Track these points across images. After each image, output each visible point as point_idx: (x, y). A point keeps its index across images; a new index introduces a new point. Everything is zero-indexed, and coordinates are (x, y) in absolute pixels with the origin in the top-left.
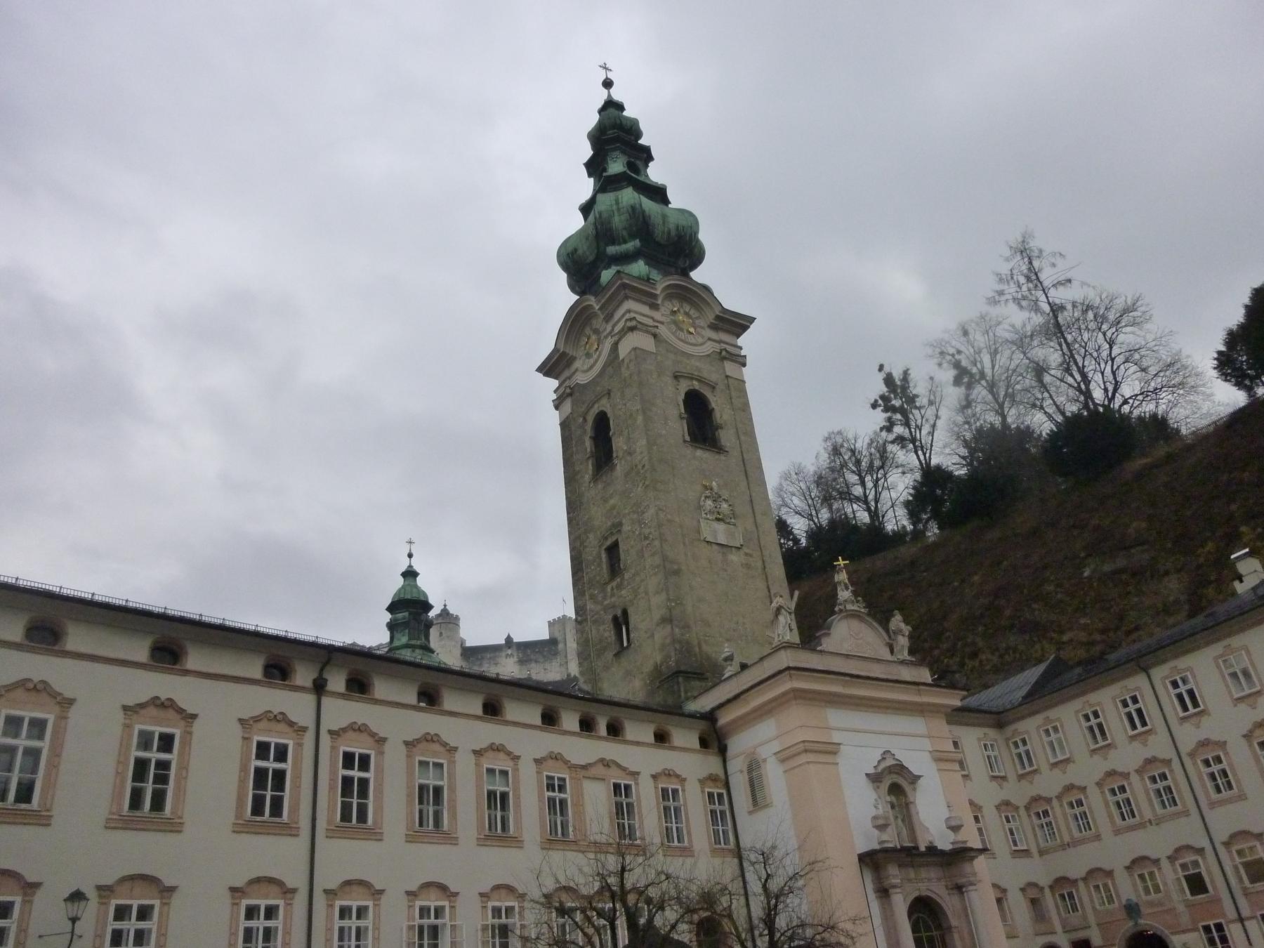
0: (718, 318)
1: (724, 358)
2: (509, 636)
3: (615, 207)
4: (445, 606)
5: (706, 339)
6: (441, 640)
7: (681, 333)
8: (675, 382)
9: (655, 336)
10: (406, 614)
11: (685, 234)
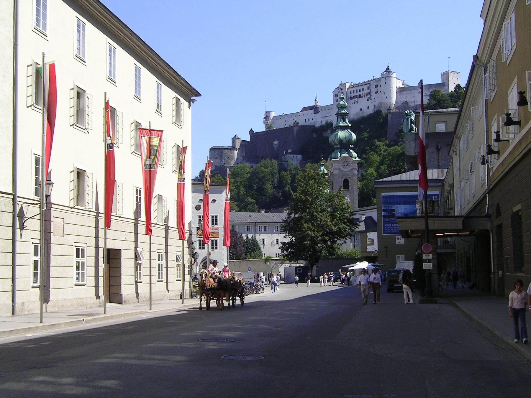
0: (352, 162)
4: (388, 66)
9: (339, 170)
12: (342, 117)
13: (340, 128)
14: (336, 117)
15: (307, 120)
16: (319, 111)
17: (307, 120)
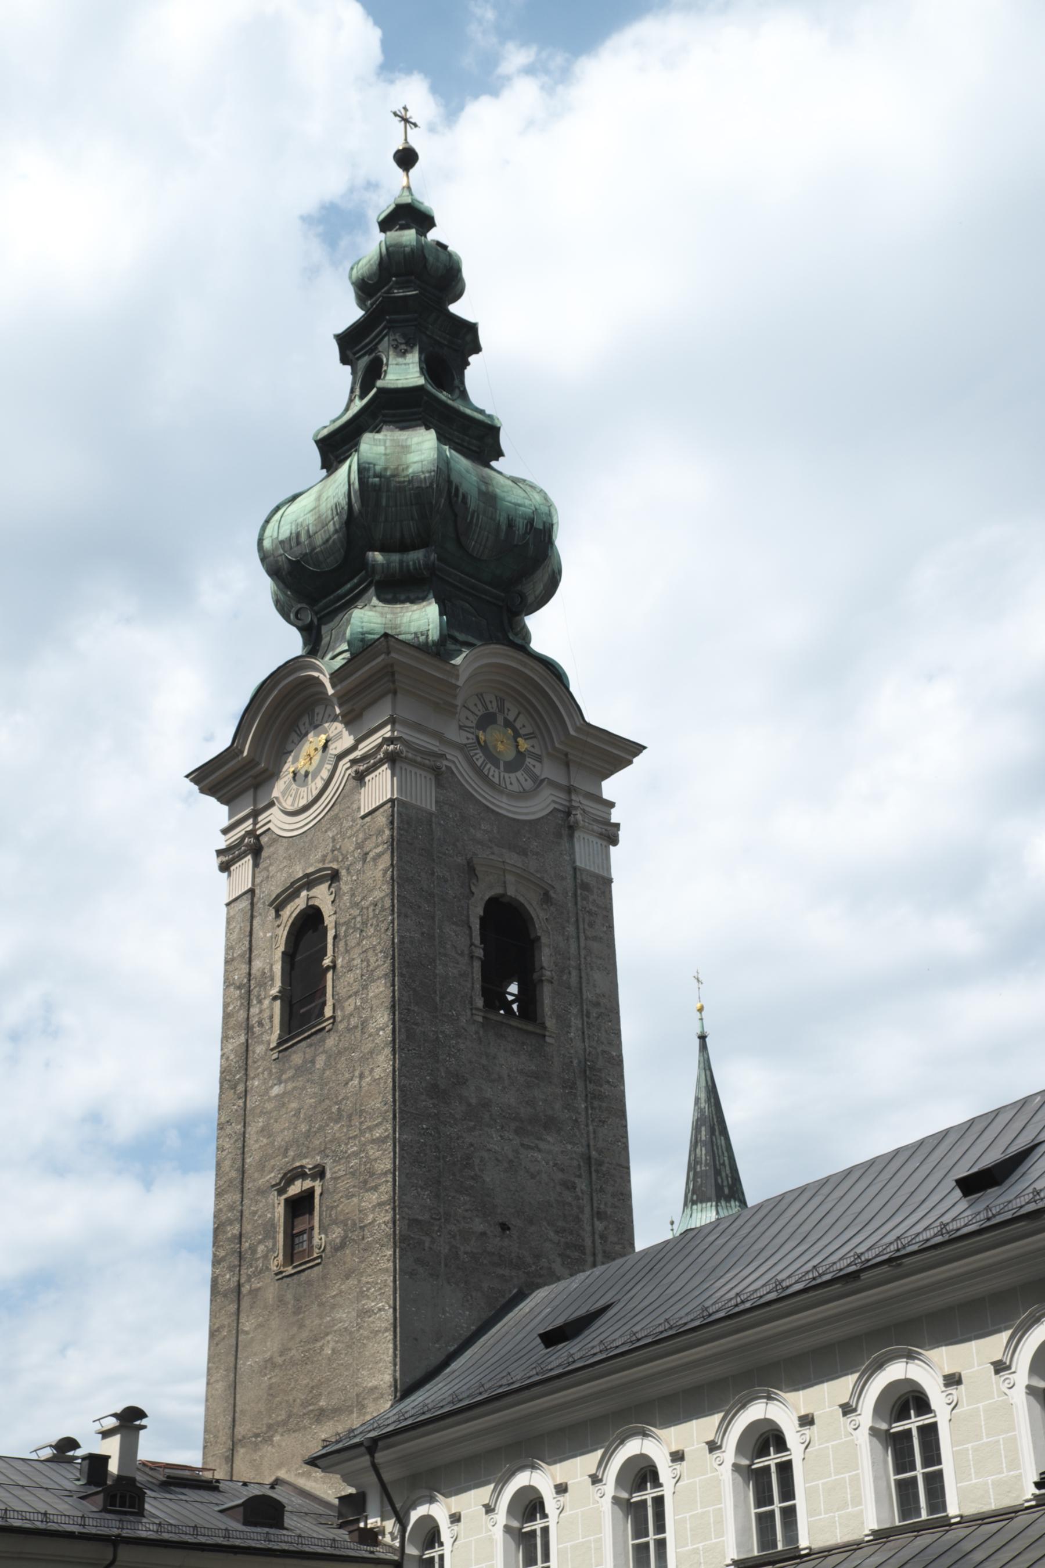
7: (493, 768)
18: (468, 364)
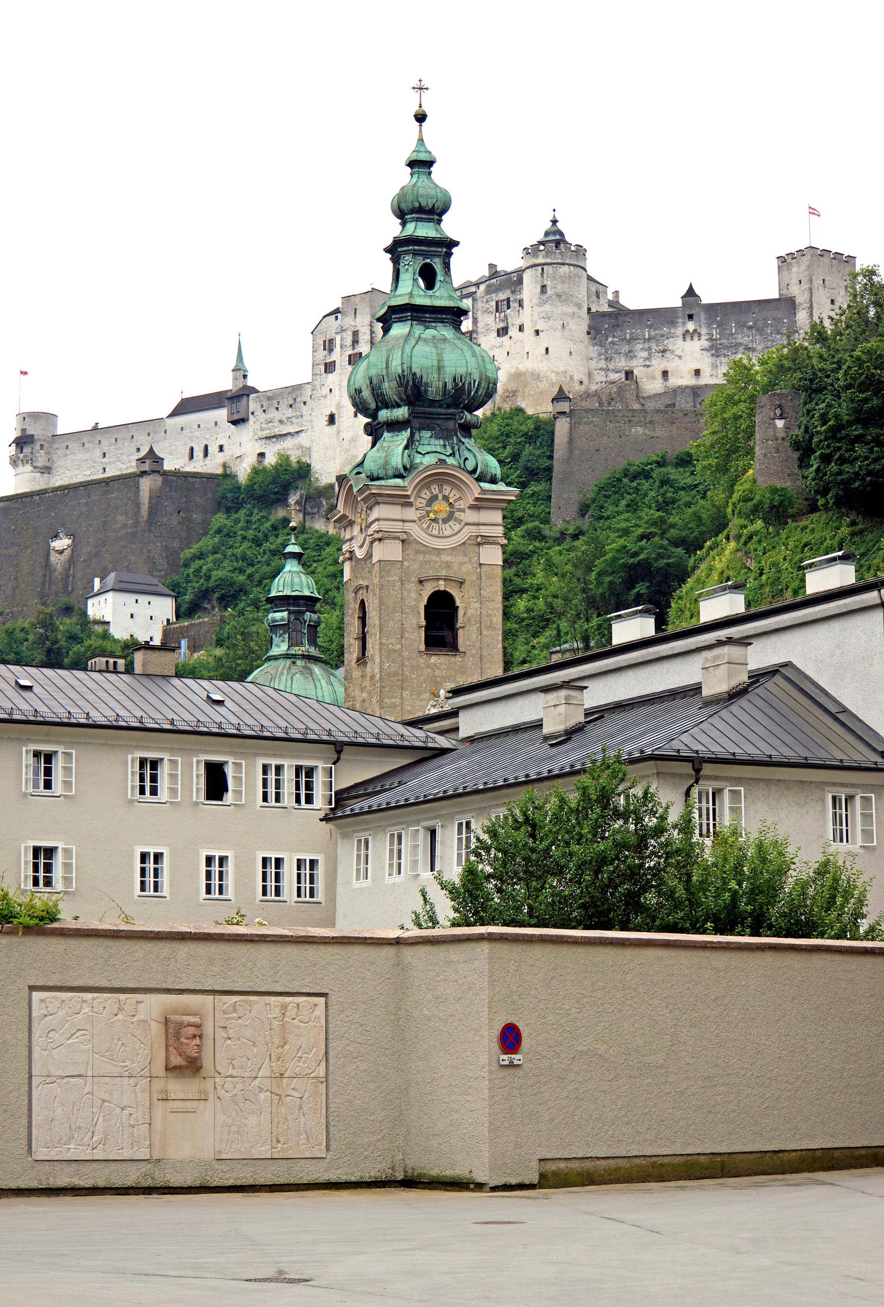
0: (477, 499)
1: (479, 544)
2: (691, 292)
3: (384, 373)
4: (554, 222)
5: (463, 524)
6: (542, 303)
8: (419, 587)
9: (403, 541)
10: (285, 614)
11: (464, 384)
12: (420, 262)
13: (412, 320)
14: (390, 265)
15: (199, 453)
16: (251, 410)
17: (199, 453)
18: (452, 254)
